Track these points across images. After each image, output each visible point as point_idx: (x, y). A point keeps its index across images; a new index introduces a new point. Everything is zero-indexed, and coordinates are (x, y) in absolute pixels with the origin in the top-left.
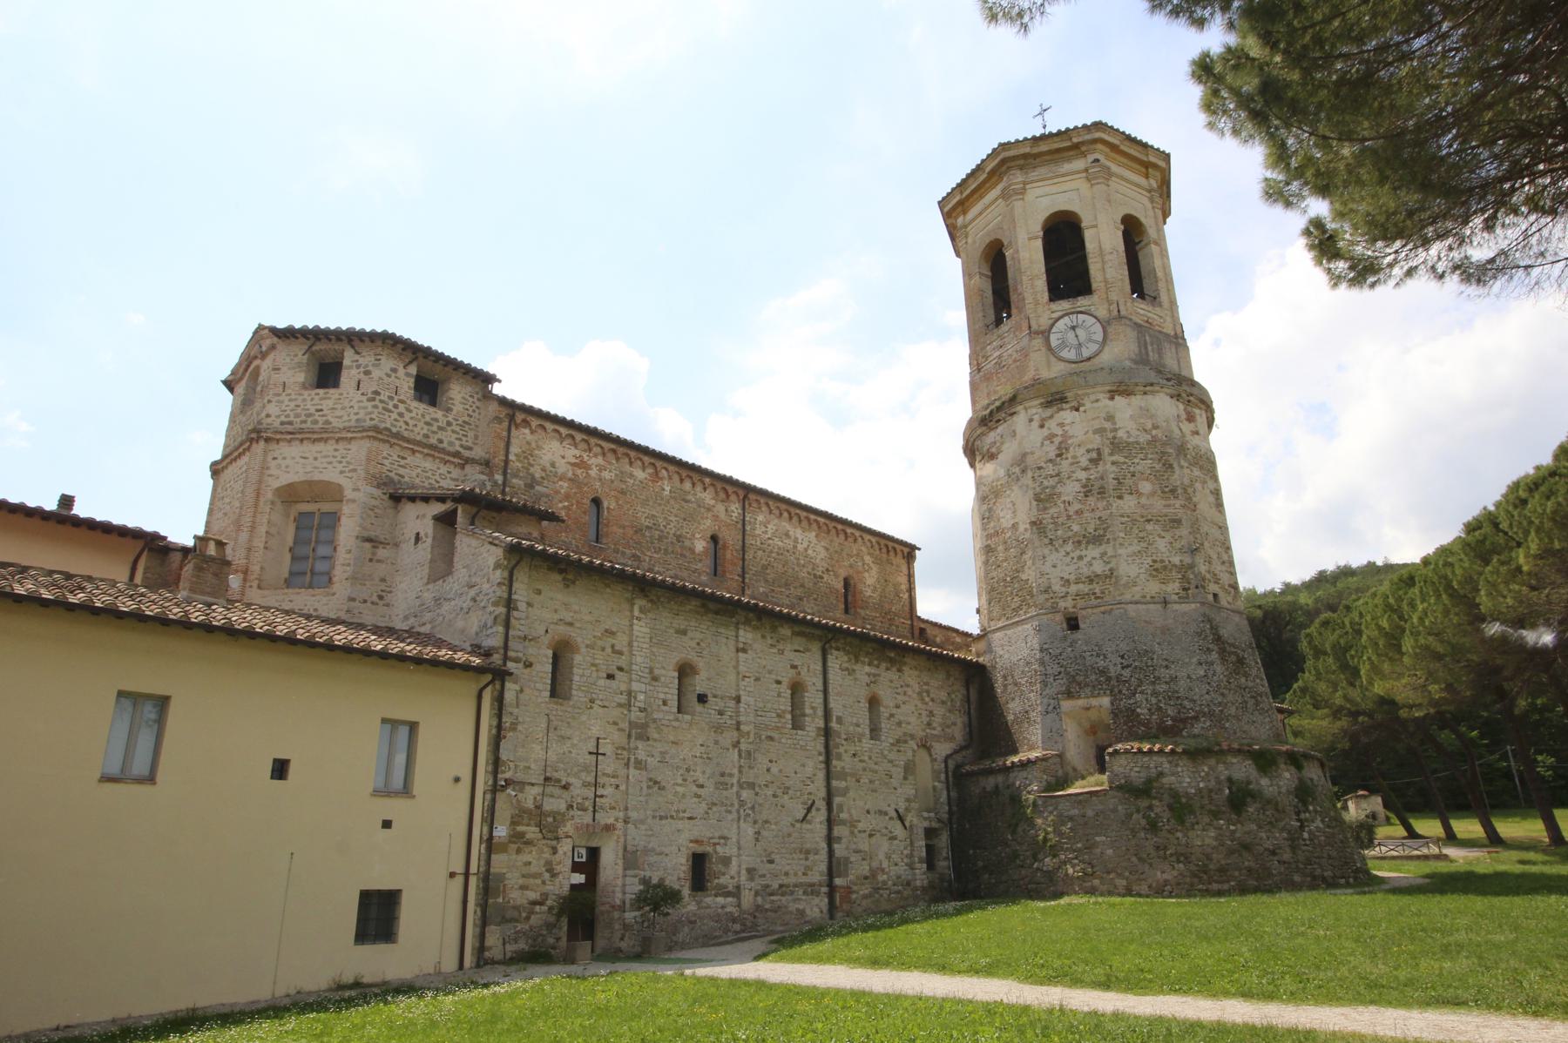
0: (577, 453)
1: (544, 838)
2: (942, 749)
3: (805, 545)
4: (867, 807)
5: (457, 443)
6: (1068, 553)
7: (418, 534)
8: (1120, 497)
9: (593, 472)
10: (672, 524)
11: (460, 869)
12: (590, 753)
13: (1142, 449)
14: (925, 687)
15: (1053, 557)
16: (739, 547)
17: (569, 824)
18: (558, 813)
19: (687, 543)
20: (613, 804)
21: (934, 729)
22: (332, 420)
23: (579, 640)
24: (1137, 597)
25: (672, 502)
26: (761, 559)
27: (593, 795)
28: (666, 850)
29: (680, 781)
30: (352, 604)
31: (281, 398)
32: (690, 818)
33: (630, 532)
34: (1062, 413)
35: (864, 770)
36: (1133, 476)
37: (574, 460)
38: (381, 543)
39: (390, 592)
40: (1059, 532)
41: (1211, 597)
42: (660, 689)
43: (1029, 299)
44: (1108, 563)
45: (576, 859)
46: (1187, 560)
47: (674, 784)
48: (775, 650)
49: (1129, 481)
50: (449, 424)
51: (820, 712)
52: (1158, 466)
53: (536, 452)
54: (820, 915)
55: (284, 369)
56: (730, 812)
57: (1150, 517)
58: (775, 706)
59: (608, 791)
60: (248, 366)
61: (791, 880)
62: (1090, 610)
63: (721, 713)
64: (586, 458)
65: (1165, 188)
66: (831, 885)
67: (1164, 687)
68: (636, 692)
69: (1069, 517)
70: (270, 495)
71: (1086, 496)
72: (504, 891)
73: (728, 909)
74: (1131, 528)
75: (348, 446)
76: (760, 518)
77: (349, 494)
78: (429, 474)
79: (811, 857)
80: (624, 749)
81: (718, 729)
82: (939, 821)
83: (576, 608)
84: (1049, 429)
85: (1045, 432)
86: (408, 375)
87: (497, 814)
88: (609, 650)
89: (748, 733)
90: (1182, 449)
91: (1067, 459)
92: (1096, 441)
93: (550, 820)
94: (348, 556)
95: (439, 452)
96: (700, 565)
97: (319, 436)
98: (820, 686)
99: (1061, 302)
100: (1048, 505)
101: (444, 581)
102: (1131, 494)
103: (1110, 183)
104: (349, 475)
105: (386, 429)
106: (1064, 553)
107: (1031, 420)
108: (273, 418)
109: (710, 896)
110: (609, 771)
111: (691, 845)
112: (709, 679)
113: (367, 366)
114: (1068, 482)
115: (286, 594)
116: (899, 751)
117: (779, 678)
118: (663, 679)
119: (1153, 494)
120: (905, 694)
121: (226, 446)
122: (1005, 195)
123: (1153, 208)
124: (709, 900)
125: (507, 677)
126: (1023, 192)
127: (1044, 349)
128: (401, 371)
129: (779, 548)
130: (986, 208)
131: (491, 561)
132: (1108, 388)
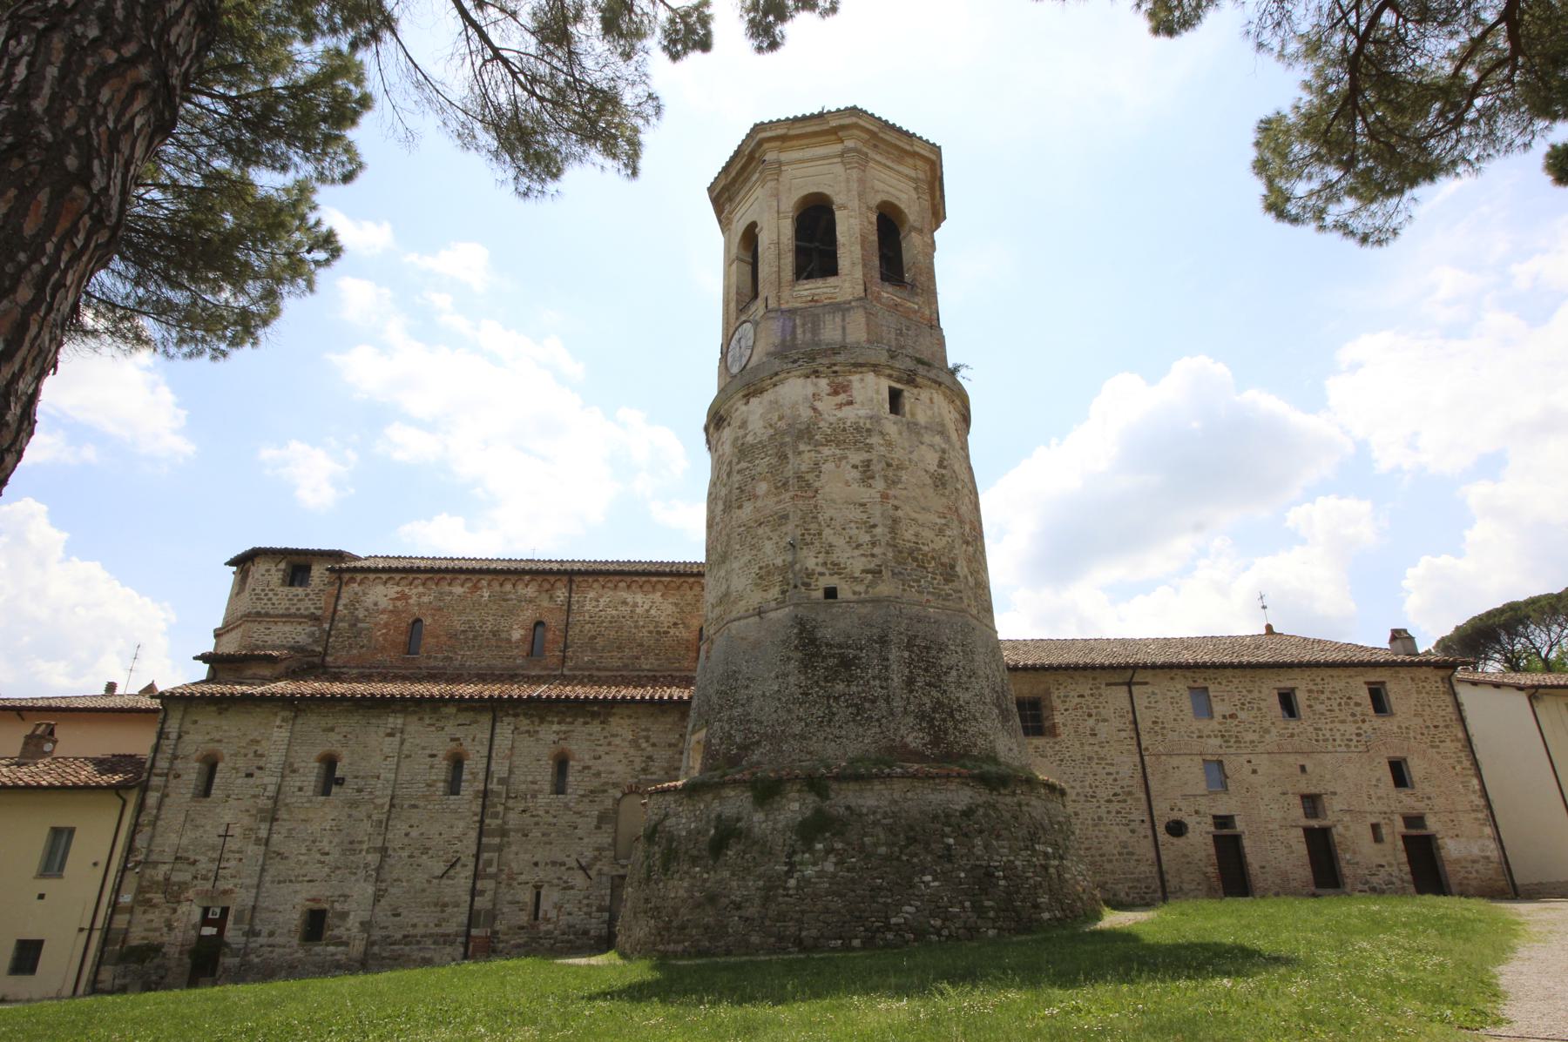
0: (399, 589)
4: (535, 859)
11: (87, 926)
19: (504, 635)
21: (652, 773)
23: (225, 751)
28: (281, 908)
29: (304, 851)
35: (537, 824)
45: (210, 916)
50: (307, 595)
51: (482, 776)
59: (233, 863)
61: (420, 930)
63: (360, 791)
66: (468, 935)
67: (740, 710)
76: (592, 594)
79: (449, 910)
83: (226, 728)
86: (278, 570)
88: (251, 755)
93: (176, 888)
110: (234, 848)
117: (434, 752)
124: (317, 949)
128: (273, 569)
132: (741, 394)
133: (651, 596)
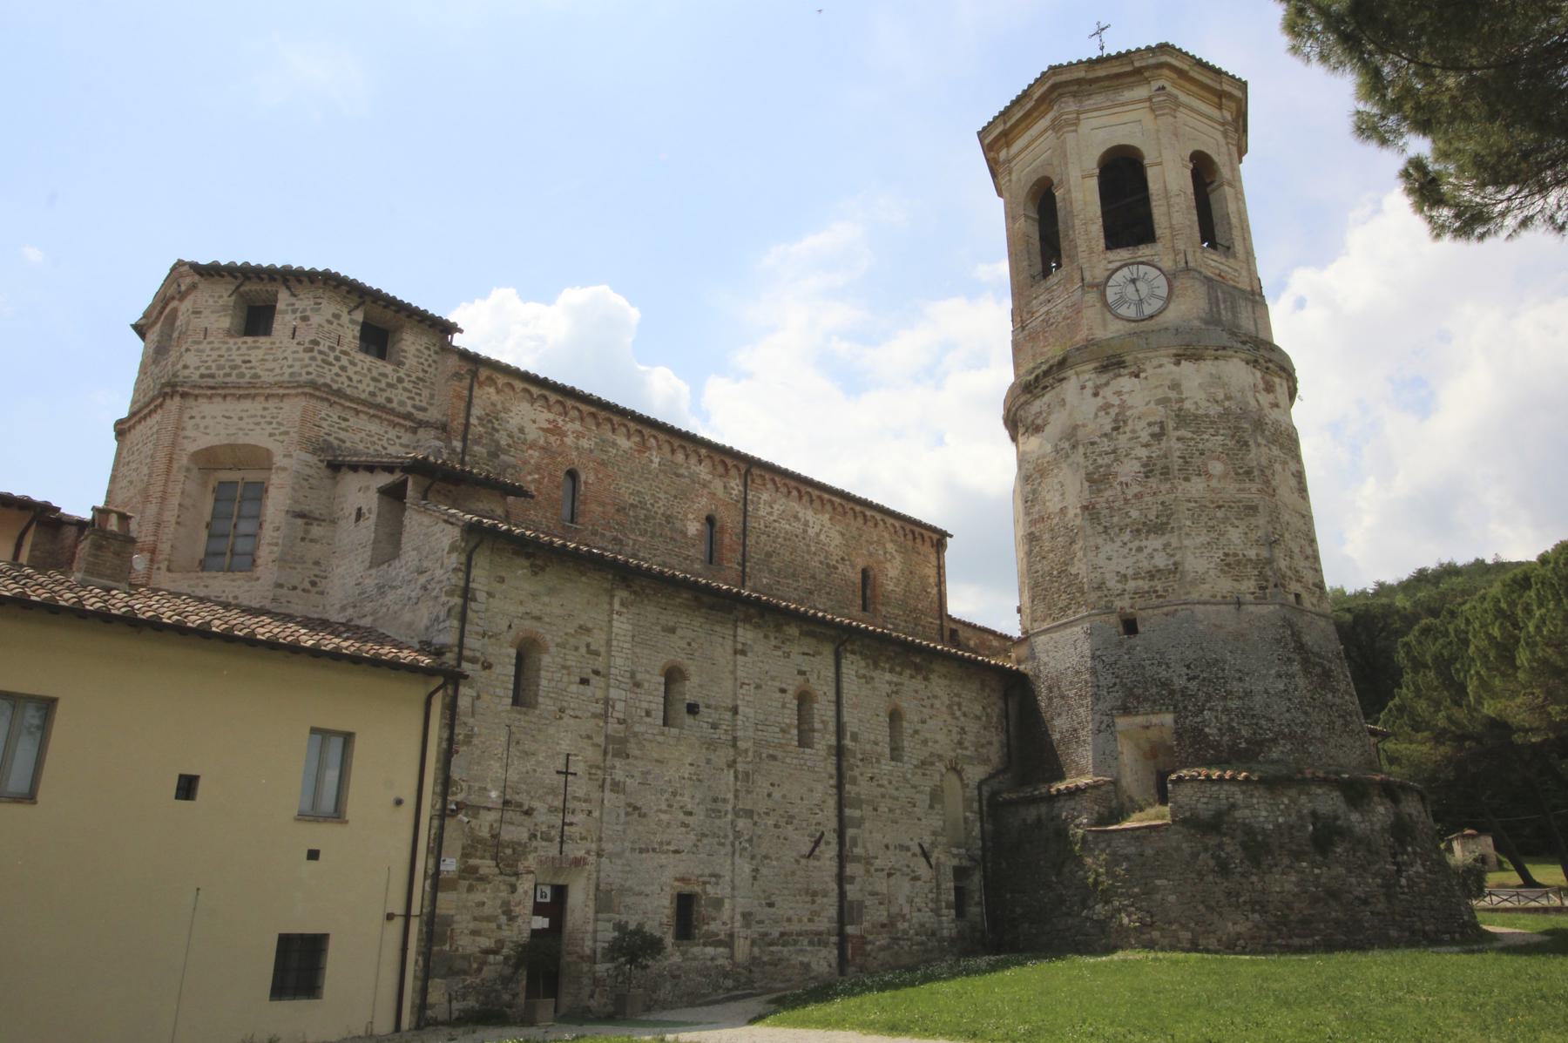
0: (551, 416)
1: (501, 873)
2: (975, 773)
3: (817, 529)
4: (886, 841)
5: (409, 403)
6: (1125, 544)
7: (360, 509)
8: (1187, 479)
9: (569, 440)
10: (661, 503)
11: (399, 909)
12: (558, 772)
13: (1213, 422)
14: (956, 699)
15: (1108, 549)
16: (739, 530)
17: (531, 857)
18: (519, 844)
20: (584, 833)
21: (966, 749)
22: (261, 373)
23: (548, 637)
24: (1206, 597)
25: (661, 476)
26: (765, 545)
27: (560, 822)
28: (648, 890)
29: (664, 807)
30: (280, 591)
31: (201, 347)
32: (676, 852)
33: (611, 510)
34: (1120, 379)
35: (883, 796)
36: (1202, 454)
37: (546, 425)
38: (316, 519)
39: (326, 578)
40: (1115, 519)
41: (1292, 598)
42: (643, 697)
43: (1082, 247)
44: (1172, 556)
45: (539, 900)
46: (1265, 553)
47: (657, 811)
48: (780, 653)
49: (1197, 461)
50: (400, 380)
51: (832, 726)
52: (1231, 444)
53: (502, 415)
54: (827, 969)
55: (206, 312)
56: (723, 845)
57: (1221, 503)
58: (779, 719)
59: (579, 818)
60: (164, 308)
62: (1150, 611)
64: (561, 423)
65: (1241, 120)
66: (841, 933)
67: (1238, 703)
68: (614, 701)
69: (1126, 501)
70: (185, 461)
71: (1147, 477)
72: (452, 938)
73: (720, 962)
74: (1200, 516)
75: (281, 405)
76: (765, 496)
77: (279, 460)
78: (375, 439)
79: (819, 900)
80: (598, 767)
81: (711, 745)
82: (971, 858)
84: (1104, 397)
85: (1100, 401)
86: (353, 322)
87: (445, 844)
88: (583, 650)
89: (746, 751)
90: (1259, 425)
91: (1125, 433)
92: (1159, 413)
93: (509, 851)
94: (275, 534)
95: (387, 413)
96: (693, 550)
97: (246, 392)
98: (832, 696)
99: (1118, 250)
100: (1103, 487)
101: (390, 565)
102: (1200, 475)
103: (1178, 114)
104: (281, 438)
105: (326, 385)
106: (1121, 544)
107: (1083, 388)
108: (192, 370)
109: (698, 945)
110: (580, 793)
111: (676, 884)
112: (700, 686)
113: (304, 310)
114: (1126, 460)
115: (201, 578)
116: (924, 775)
117: (784, 686)
118: (646, 685)
119: (1225, 475)
120: (932, 706)
121: (134, 402)
122: (1055, 126)
123: (1227, 144)
124: (696, 950)
125: (462, 681)
126: (1076, 123)
127: (1099, 305)
128: (345, 318)
129: (787, 533)
130: (1034, 141)
131: (446, 543)
132: (1174, 351)
133: (819, 516)
